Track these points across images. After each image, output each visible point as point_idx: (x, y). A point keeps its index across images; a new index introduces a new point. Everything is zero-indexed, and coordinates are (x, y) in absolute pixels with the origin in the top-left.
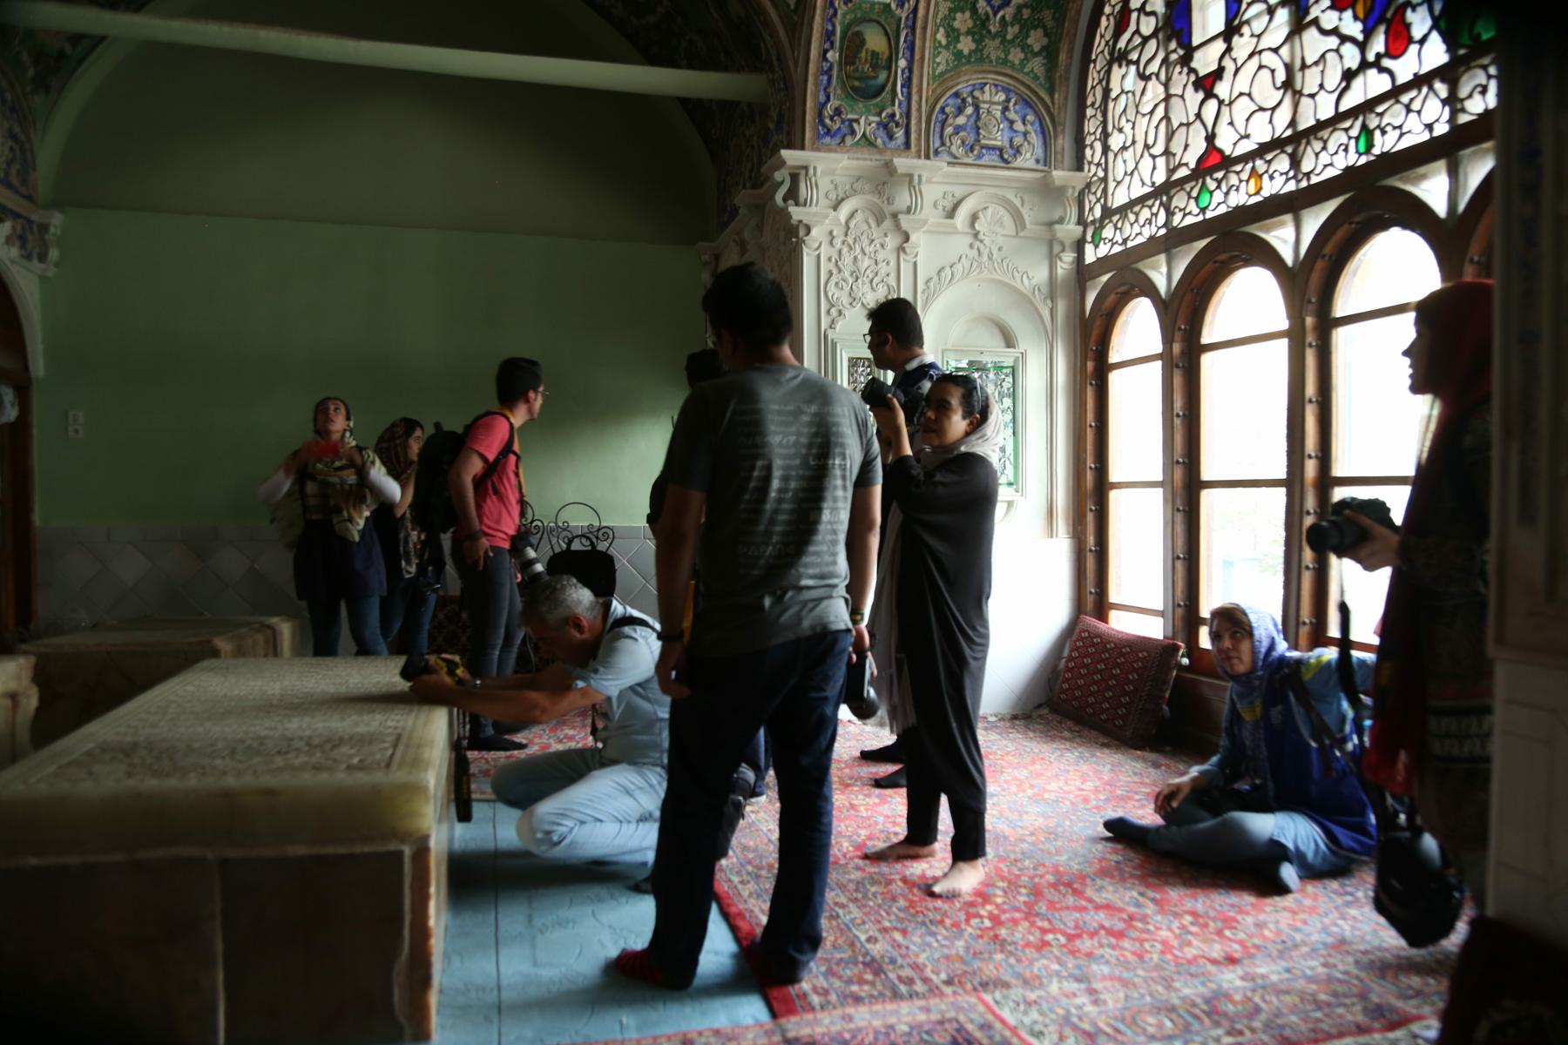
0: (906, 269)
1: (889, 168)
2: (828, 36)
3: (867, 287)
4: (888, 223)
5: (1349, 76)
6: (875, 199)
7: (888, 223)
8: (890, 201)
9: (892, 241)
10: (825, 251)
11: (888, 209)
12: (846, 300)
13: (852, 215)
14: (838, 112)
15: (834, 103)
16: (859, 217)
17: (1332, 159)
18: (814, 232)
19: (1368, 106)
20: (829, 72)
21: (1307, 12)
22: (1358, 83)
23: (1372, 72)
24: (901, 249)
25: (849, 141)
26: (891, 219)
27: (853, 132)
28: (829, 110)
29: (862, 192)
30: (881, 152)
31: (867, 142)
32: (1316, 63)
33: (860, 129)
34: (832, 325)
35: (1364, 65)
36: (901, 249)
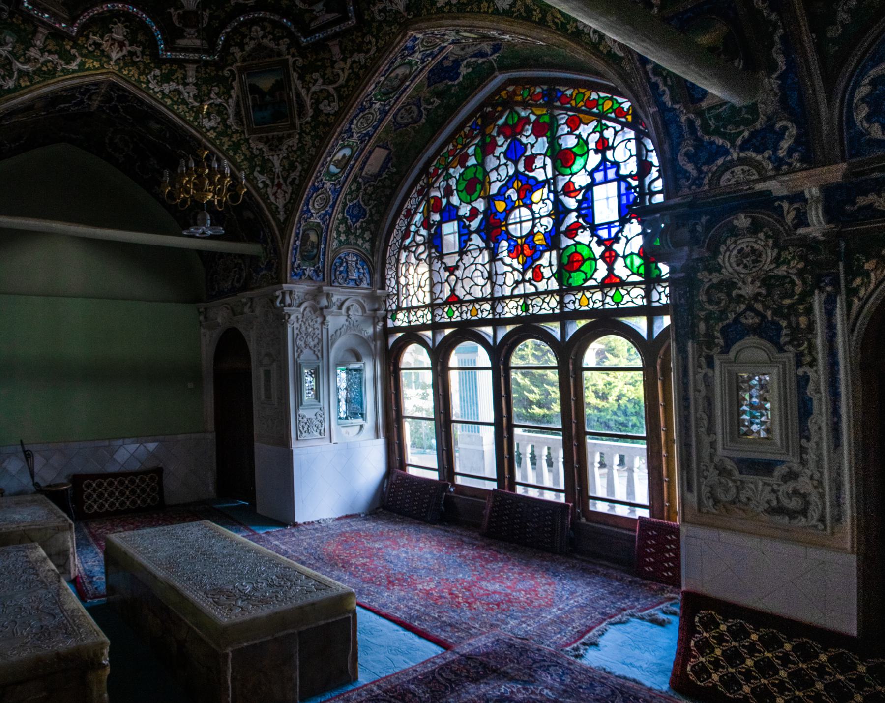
0: (324, 331)
1: (319, 290)
2: (297, 234)
3: (311, 340)
4: (318, 312)
5: (517, 283)
6: (312, 302)
7: (318, 312)
8: (318, 303)
9: (319, 320)
10: (296, 325)
11: (318, 306)
12: (303, 346)
13: (305, 310)
14: (299, 266)
15: (298, 262)
16: (308, 310)
17: (511, 309)
18: (292, 317)
19: (526, 296)
20: (296, 249)
21: (497, 255)
22: (521, 286)
23: (527, 284)
24: (323, 323)
25: (303, 278)
26: (321, 312)
27: (304, 274)
28: (296, 265)
29: (308, 300)
30: (315, 282)
31: (310, 278)
32: (502, 274)
33: (307, 272)
34: (299, 357)
35: (523, 281)
36: (323, 323)
